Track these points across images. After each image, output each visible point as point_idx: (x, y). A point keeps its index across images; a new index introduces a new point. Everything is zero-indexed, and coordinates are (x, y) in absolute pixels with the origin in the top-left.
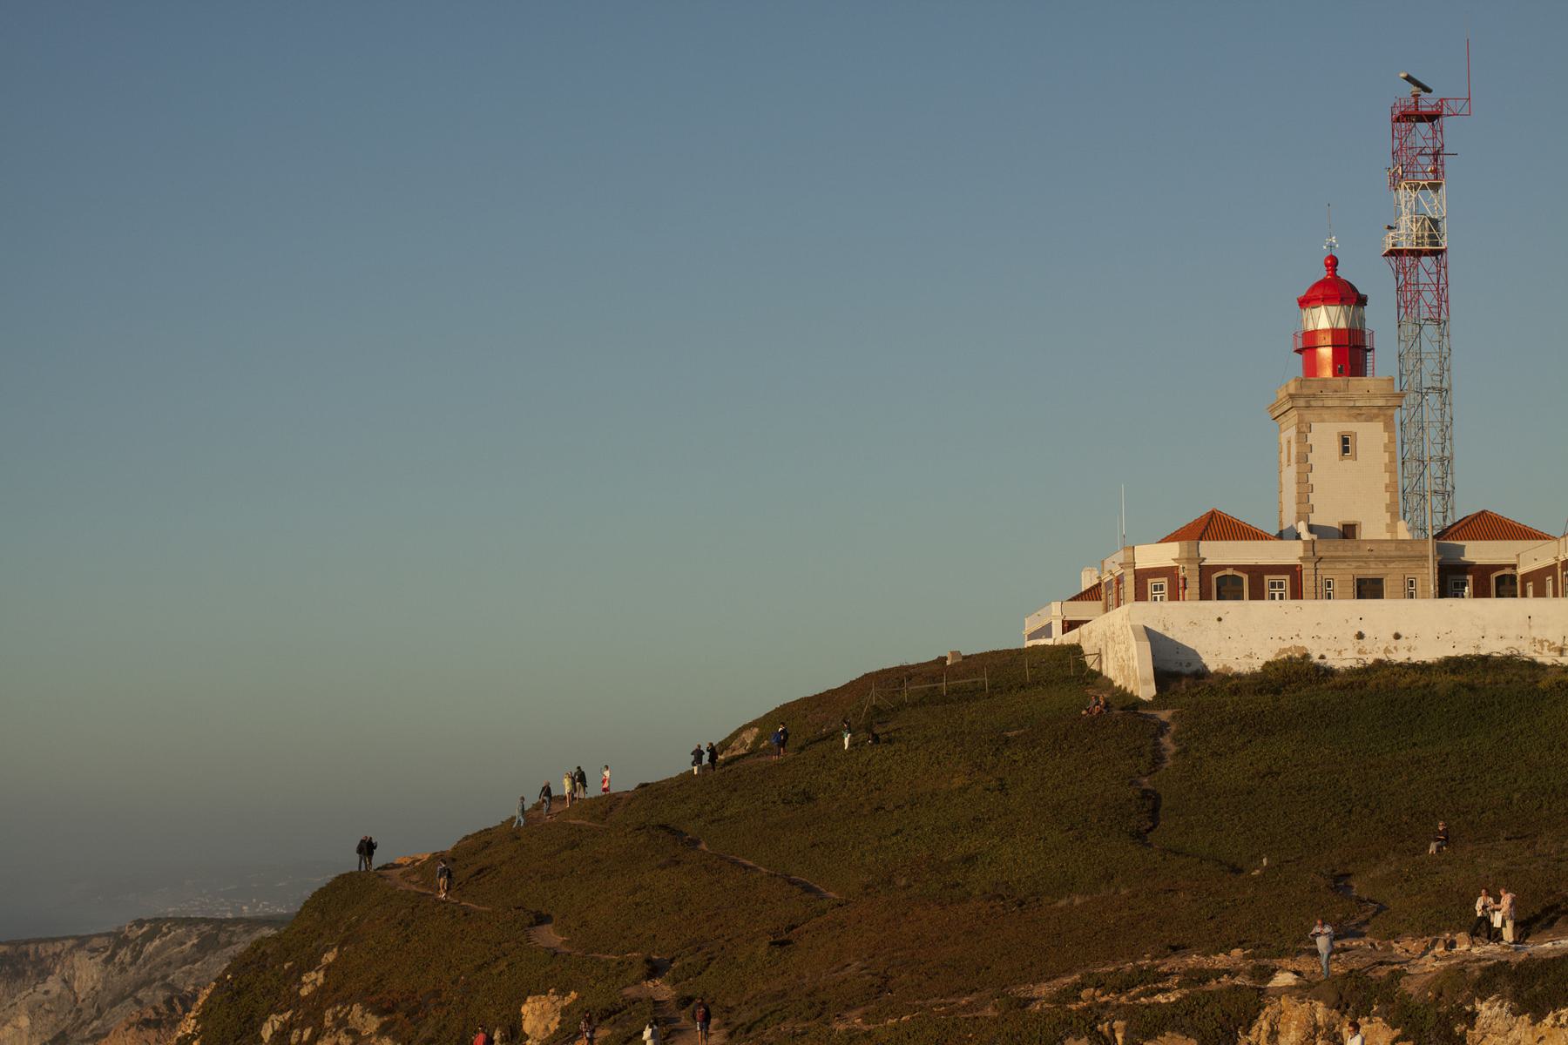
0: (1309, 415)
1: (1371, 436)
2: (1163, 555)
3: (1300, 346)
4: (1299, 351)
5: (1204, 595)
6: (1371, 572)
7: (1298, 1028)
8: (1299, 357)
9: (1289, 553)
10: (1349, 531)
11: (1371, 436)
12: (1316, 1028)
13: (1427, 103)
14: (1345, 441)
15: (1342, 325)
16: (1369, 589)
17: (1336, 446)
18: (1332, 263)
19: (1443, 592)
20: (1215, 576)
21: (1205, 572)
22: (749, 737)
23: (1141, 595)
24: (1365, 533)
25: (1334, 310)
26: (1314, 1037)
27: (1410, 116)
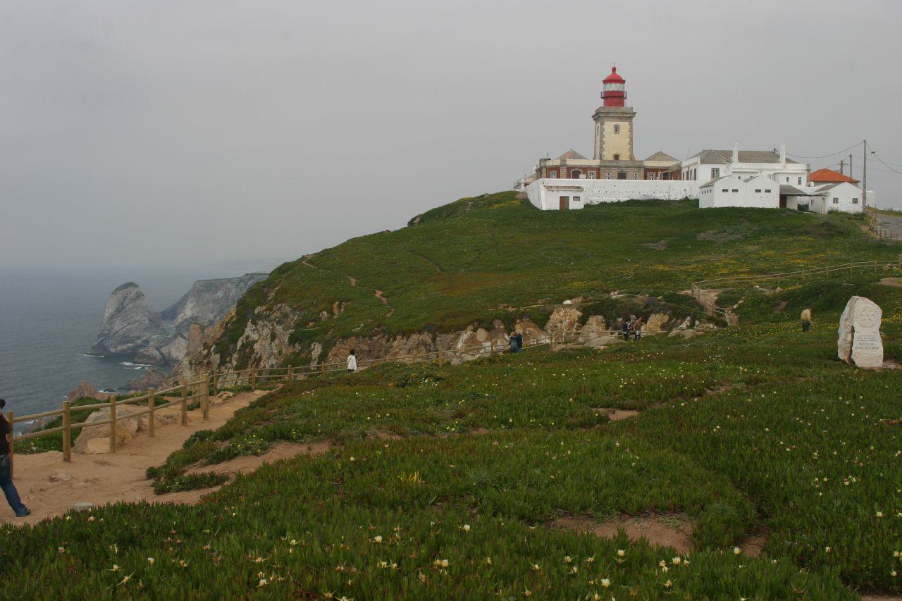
1: (624, 125)
2: (557, 163)
3: (603, 96)
5: (568, 177)
6: (625, 170)
8: (602, 100)
9: (596, 163)
14: (616, 128)
16: (622, 176)
17: (613, 130)
18: (614, 70)
19: (645, 178)
20: (572, 171)
21: (569, 168)
22: (418, 220)
23: (548, 176)
24: (620, 158)
25: (613, 85)
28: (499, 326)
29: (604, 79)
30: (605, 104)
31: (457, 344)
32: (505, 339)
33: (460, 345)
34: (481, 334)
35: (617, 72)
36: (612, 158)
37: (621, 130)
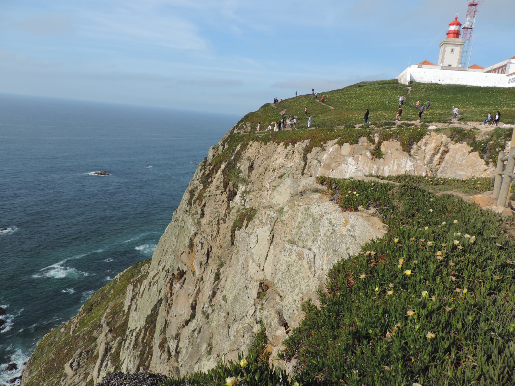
0: (446, 45)
1: (457, 49)
4: (447, 34)
7: (435, 143)
10: (450, 66)
11: (457, 49)
12: (442, 143)
13: (475, 3)
15: (456, 29)
17: (451, 51)
18: (457, 18)
24: (452, 66)
26: (440, 146)
27: (472, 5)
28: (363, 142)
29: (449, 23)
30: (448, 37)
31: (323, 155)
32: (367, 156)
33: (325, 156)
34: (347, 148)
35: (458, 20)
36: (447, 66)
37: (455, 51)
